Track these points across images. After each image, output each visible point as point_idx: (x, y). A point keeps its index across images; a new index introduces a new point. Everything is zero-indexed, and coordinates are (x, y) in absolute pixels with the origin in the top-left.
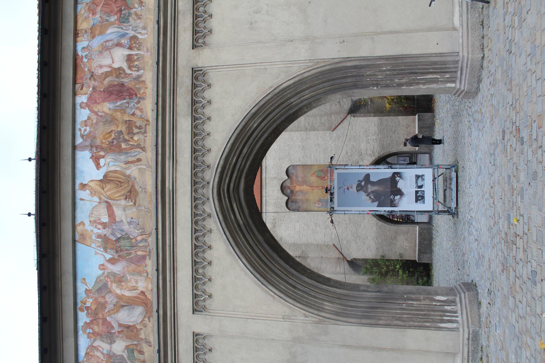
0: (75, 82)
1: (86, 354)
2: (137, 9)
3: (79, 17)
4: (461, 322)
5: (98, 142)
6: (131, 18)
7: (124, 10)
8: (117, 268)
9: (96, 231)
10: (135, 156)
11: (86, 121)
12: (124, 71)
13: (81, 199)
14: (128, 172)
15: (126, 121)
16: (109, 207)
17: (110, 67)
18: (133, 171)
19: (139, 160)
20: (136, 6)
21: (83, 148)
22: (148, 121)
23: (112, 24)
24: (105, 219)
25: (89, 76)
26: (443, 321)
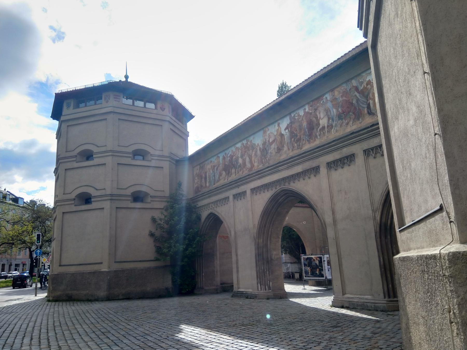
0: (312, 101)
3: (340, 87)
4: (261, 291)
5: (293, 126)
6: (340, 120)
7: (344, 115)
8: (259, 152)
9: (267, 137)
10: (290, 147)
11: (299, 115)
12: (318, 128)
13: (275, 126)
14: (285, 146)
15: (301, 137)
16: (274, 141)
17: (320, 118)
18: (285, 148)
19: (289, 149)
20: (346, 121)
22: (302, 148)
23: (337, 110)
25: (316, 108)
26: (261, 285)
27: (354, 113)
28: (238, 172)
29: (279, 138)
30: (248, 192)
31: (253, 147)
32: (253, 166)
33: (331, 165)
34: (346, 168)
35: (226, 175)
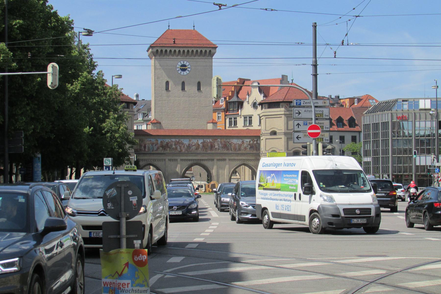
1: (172, 141)
2: (224, 149)
8: (186, 147)
18: (200, 149)
21: (203, 140)
23: (222, 145)
24: (193, 145)
27: (227, 148)
28: (172, 150)
29: (197, 145)
30: (179, 160)
31: (183, 144)
32: (181, 150)
33: (218, 160)
34: (222, 162)
35: (163, 149)
